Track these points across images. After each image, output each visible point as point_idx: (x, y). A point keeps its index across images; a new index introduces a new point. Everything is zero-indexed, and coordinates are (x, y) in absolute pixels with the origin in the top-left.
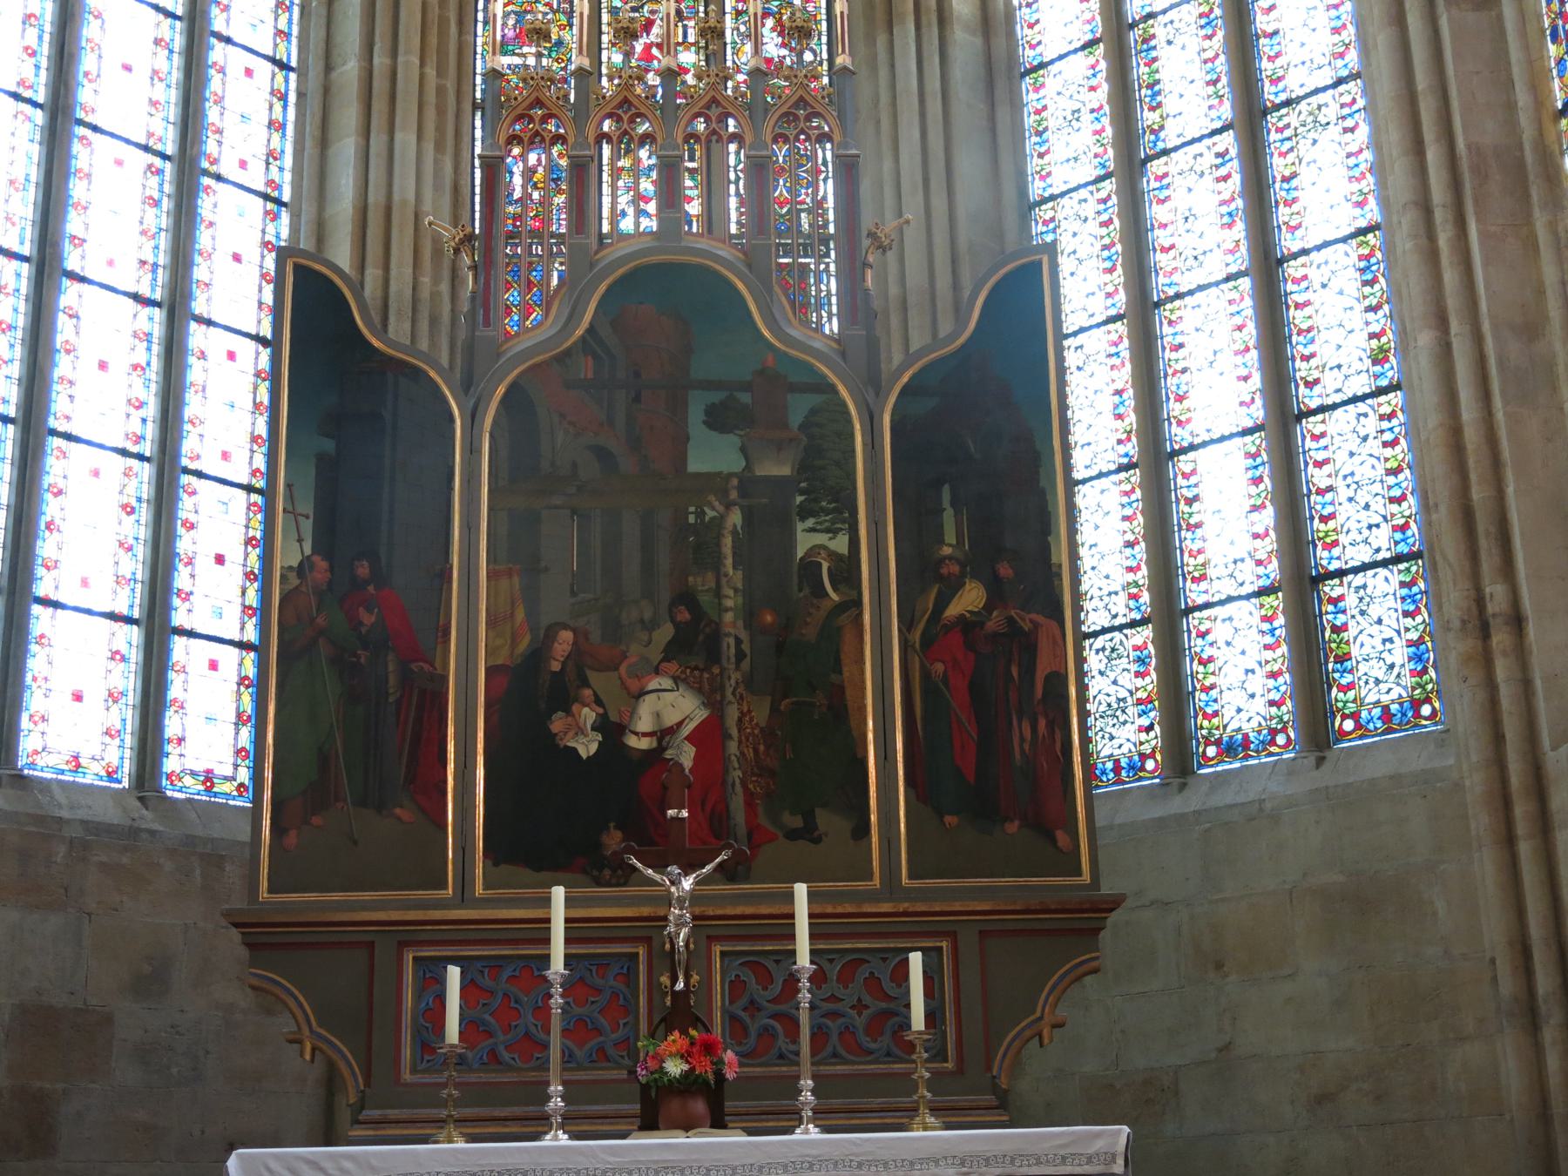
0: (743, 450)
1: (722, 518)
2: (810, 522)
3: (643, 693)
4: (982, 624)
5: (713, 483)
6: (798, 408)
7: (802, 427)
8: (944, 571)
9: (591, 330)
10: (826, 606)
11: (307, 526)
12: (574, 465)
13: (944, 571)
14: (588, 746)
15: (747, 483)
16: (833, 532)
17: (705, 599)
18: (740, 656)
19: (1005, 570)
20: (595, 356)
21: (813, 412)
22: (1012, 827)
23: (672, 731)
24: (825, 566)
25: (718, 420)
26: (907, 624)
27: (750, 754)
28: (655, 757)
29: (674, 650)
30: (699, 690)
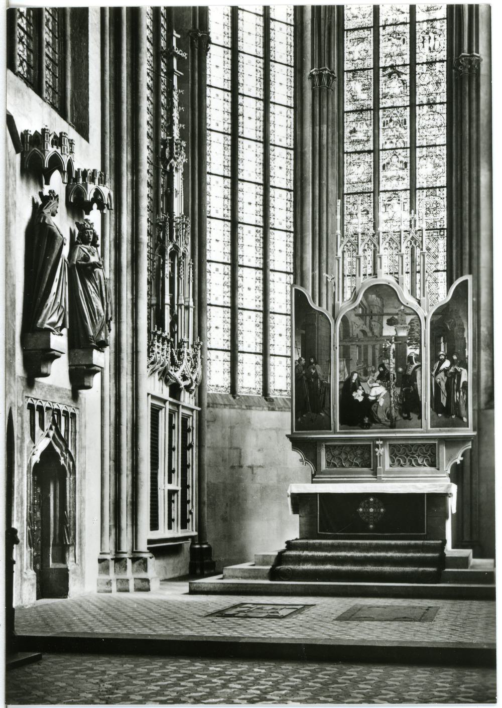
0: (395, 330)
1: (390, 346)
2: (411, 347)
3: (373, 387)
4: (449, 370)
5: (389, 339)
6: (409, 319)
7: (409, 324)
8: (441, 358)
9: (361, 302)
10: (414, 366)
11: (300, 351)
12: (357, 335)
13: (441, 358)
14: (361, 399)
15: (397, 338)
16: (415, 349)
17: (386, 365)
18: (394, 378)
19: (455, 357)
20: (362, 308)
21: (412, 320)
22: (454, 417)
23: (379, 396)
24: (414, 357)
25: (391, 322)
26: (432, 370)
27: (396, 400)
28: (375, 401)
29: (379, 378)
30: (385, 386)
